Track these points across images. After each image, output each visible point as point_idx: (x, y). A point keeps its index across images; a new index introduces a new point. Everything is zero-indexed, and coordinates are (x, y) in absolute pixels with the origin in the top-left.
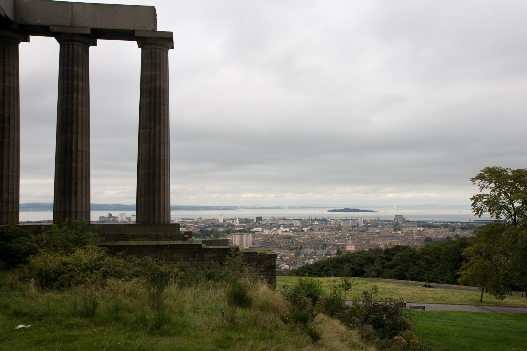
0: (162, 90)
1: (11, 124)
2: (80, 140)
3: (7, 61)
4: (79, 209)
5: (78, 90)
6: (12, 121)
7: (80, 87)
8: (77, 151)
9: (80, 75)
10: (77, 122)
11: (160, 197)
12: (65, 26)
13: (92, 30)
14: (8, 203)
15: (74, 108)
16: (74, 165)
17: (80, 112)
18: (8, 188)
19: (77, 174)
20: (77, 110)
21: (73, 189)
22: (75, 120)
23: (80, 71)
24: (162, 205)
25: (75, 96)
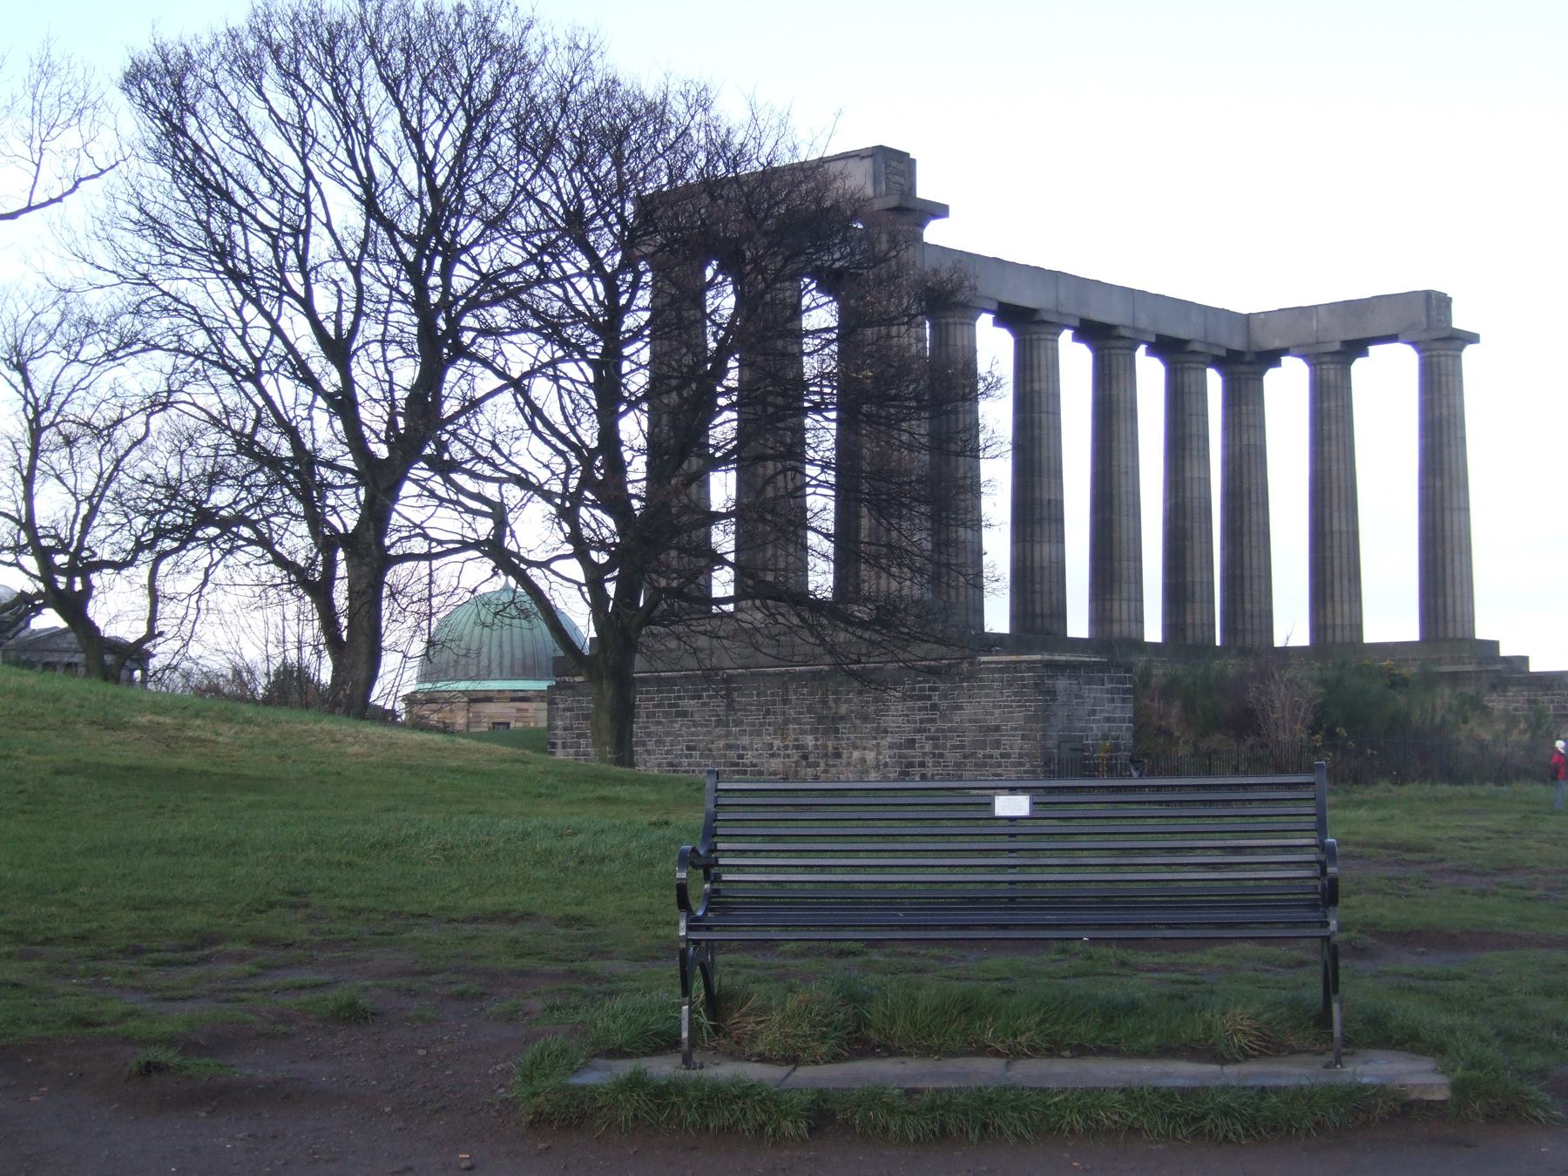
0: (1444, 423)
1: (1254, 499)
2: (1335, 514)
3: (1244, 408)
4: (1338, 621)
5: (1330, 438)
6: (1253, 496)
7: (1334, 433)
8: (1332, 532)
9: (1333, 413)
10: (1331, 488)
11: (1445, 596)
12: (1308, 345)
13: (1344, 343)
14: (1252, 616)
15: (1326, 467)
16: (1328, 554)
17: (1334, 473)
18: (1252, 595)
19: (1332, 568)
20: (1330, 469)
21: (1328, 591)
22: (1326, 485)
23: (1333, 409)
24: (1450, 610)
25: (1326, 448)
